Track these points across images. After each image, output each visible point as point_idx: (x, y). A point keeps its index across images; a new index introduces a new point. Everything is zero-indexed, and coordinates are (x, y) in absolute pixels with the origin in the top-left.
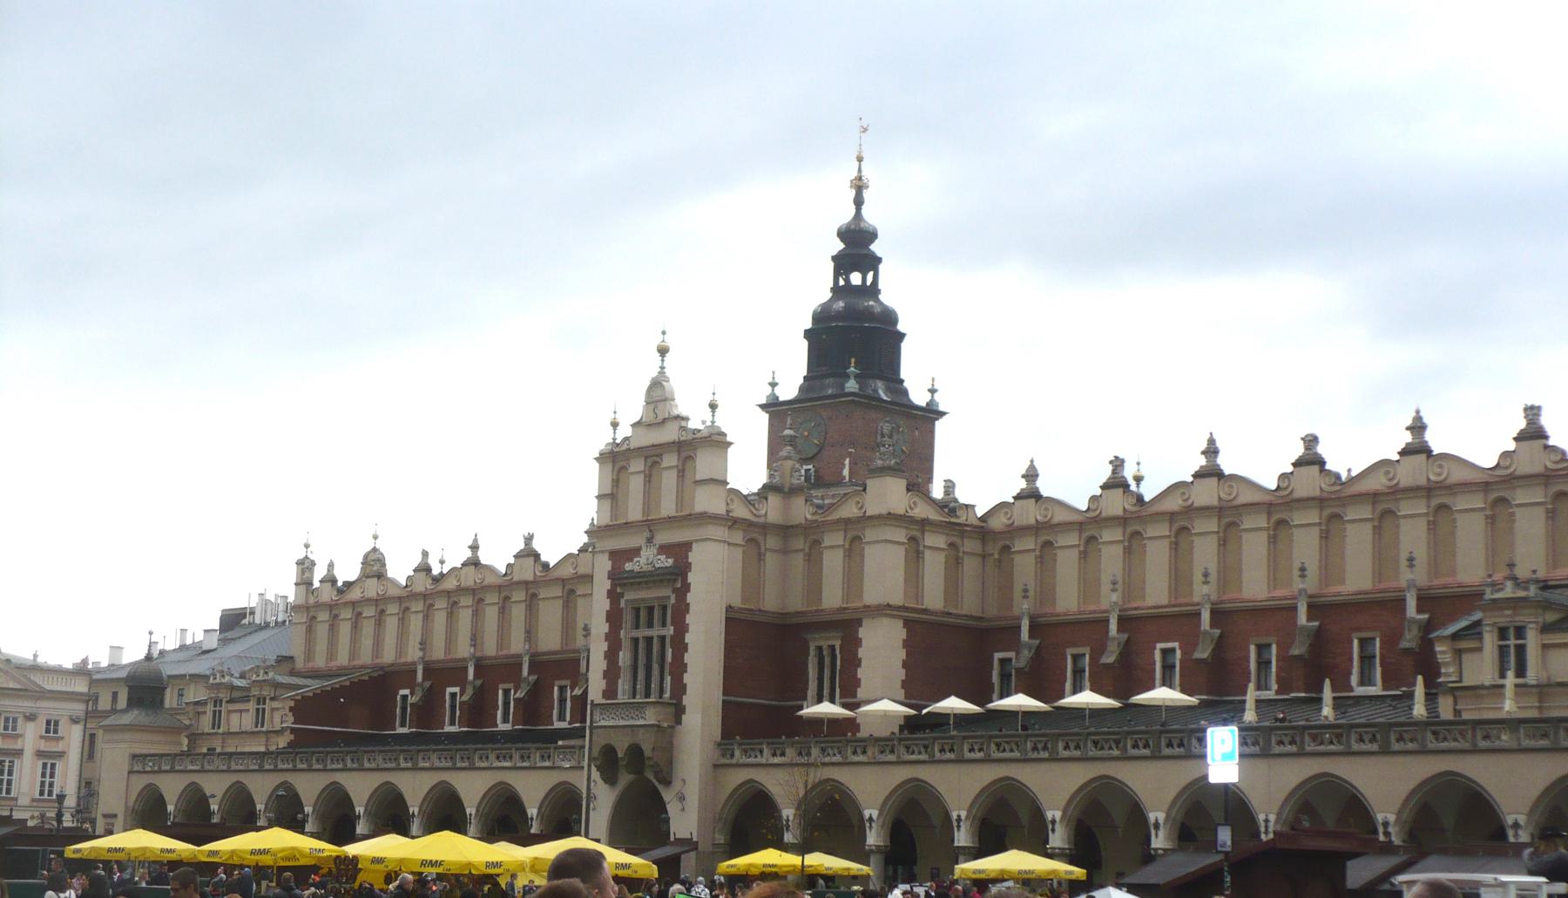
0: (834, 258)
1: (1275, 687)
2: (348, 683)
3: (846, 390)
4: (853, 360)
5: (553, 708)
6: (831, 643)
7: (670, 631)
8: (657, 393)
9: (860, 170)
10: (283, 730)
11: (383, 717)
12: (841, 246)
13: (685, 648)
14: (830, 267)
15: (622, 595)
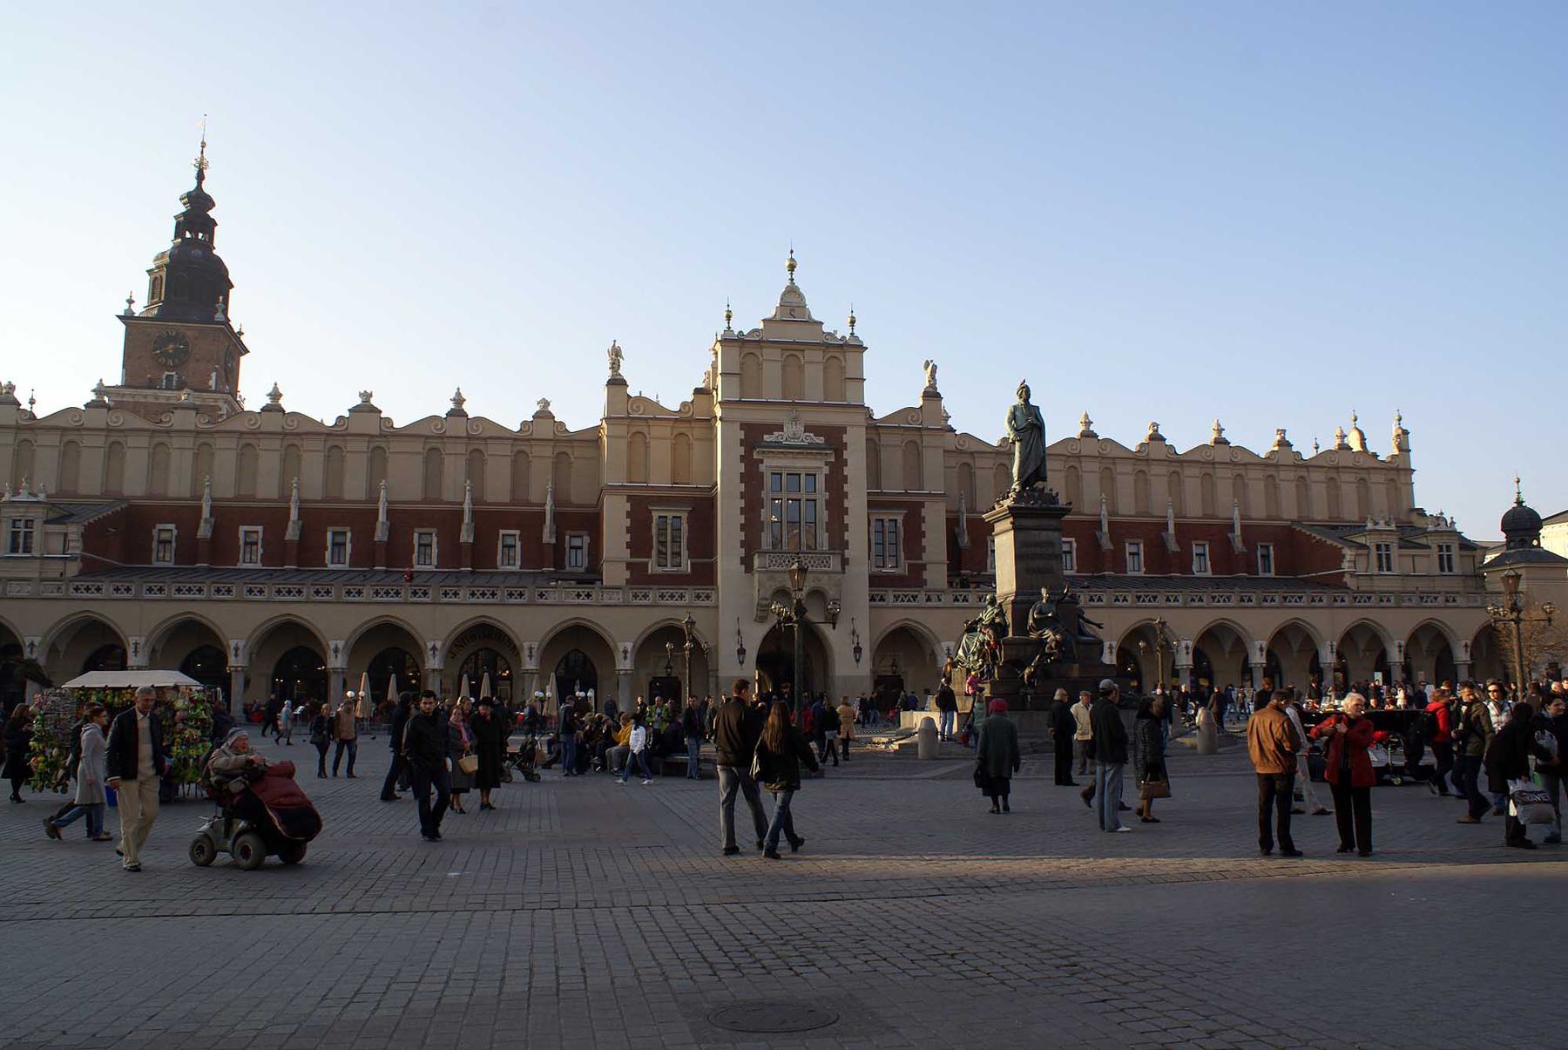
0: (176, 217)
1: (1144, 569)
2: (110, 513)
3: (216, 320)
4: (221, 298)
5: (413, 552)
6: (891, 518)
7: (822, 496)
8: (792, 299)
9: (202, 152)
10: (73, 559)
11: (143, 553)
12: (183, 209)
13: (846, 511)
14: (174, 222)
15: (762, 461)
